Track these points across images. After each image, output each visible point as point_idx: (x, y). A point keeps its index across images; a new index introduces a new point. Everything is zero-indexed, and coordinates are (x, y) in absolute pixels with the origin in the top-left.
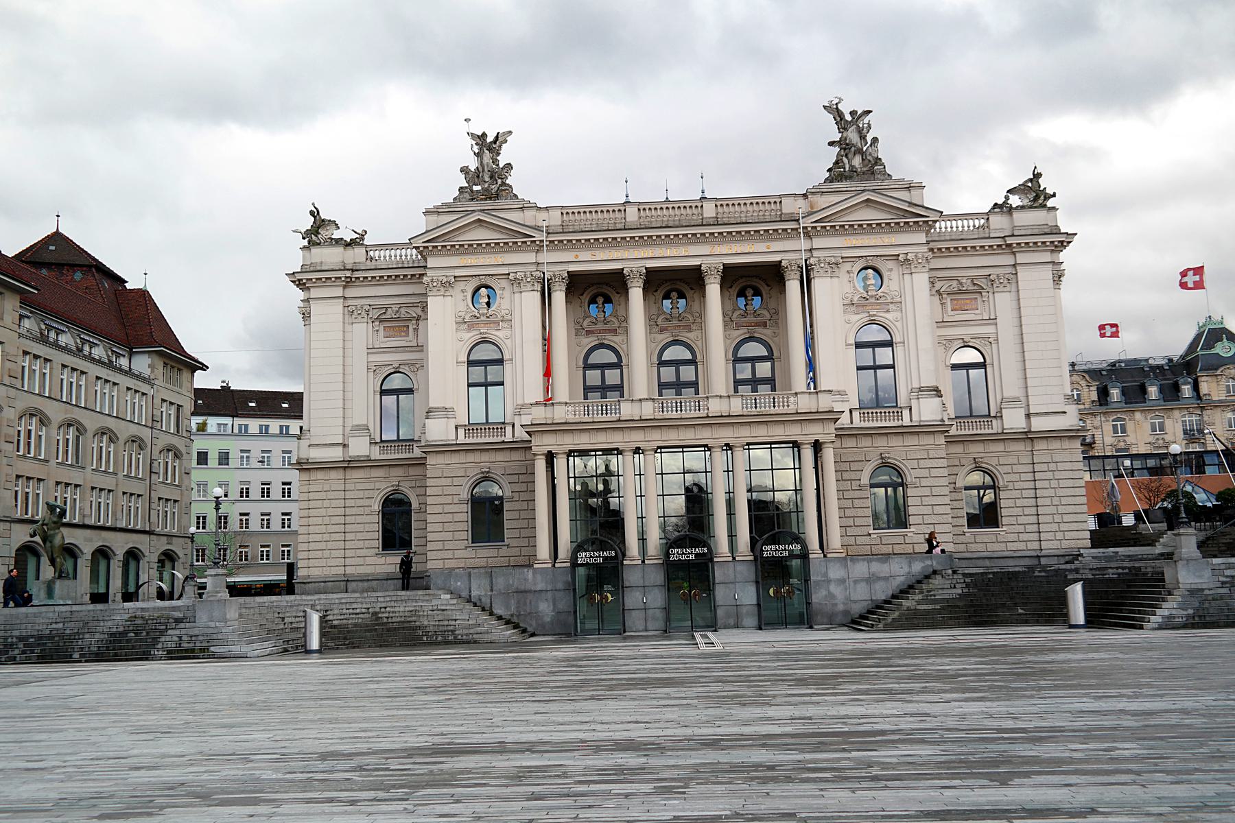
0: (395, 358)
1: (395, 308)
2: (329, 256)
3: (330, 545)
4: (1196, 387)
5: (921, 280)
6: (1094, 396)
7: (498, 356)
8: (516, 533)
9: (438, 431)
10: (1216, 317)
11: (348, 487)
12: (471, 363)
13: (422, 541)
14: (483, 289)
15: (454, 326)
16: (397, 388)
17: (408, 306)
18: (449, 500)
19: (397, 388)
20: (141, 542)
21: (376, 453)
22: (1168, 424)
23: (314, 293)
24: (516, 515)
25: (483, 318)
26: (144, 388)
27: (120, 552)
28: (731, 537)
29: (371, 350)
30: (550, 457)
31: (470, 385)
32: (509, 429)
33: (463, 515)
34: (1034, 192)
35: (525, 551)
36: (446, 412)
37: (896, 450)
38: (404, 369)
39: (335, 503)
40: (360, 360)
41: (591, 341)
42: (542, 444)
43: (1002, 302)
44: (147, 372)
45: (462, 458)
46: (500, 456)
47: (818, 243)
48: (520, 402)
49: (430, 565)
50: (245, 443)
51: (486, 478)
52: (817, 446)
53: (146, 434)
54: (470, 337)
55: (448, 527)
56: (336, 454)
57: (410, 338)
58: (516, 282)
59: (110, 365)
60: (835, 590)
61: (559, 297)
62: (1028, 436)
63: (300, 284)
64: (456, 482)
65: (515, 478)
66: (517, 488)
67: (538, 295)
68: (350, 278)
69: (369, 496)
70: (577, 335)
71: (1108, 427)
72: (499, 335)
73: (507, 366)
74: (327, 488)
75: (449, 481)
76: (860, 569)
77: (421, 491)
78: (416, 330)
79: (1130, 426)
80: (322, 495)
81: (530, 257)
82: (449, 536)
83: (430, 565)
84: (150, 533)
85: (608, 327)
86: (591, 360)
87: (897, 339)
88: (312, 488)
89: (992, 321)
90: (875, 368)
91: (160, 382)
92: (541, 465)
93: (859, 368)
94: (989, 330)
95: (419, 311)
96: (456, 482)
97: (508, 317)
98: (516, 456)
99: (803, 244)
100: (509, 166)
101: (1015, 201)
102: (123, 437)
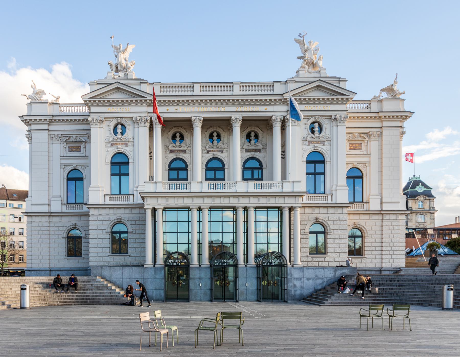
0: (73, 163)
1: (74, 136)
3: (42, 253)
7: (127, 161)
8: (134, 250)
11: (52, 225)
12: (113, 164)
13: (87, 253)
15: (105, 144)
17: (81, 136)
18: (100, 232)
24: (134, 241)
25: (119, 140)
31: (112, 175)
32: (131, 197)
35: (138, 259)
38: (79, 168)
39: (44, 233)
40: (57, 162)
41: (173, 156)
42: (149, 203)
46: (127, 211)
48: (137, 184)
49: (91, 264)
51: (119, 222)
54: (113, 150)
55: (100, 245)
56: (45, 209)
57: (82, 152)
64: (104, 223)
65: (134, 222)
66: (134, 227)
67: (147, 129)
70: (165, 152)
73: (131, 166)
74: (40, 225)
75: (100, 223)
77: (85, 228)
78: (85, 148)
80: (38, 229)
82: (100, 250)
83: (91, 264)
85: (182, 149)
86: (173, 166)
87: (327, 159)
88: (33, 225)
89: (368, 155)
90: (315, 174)
93: (307, 174)
95: (86, 138)
96: (104, 223)
97: (132, 140)
98: (135, 211)
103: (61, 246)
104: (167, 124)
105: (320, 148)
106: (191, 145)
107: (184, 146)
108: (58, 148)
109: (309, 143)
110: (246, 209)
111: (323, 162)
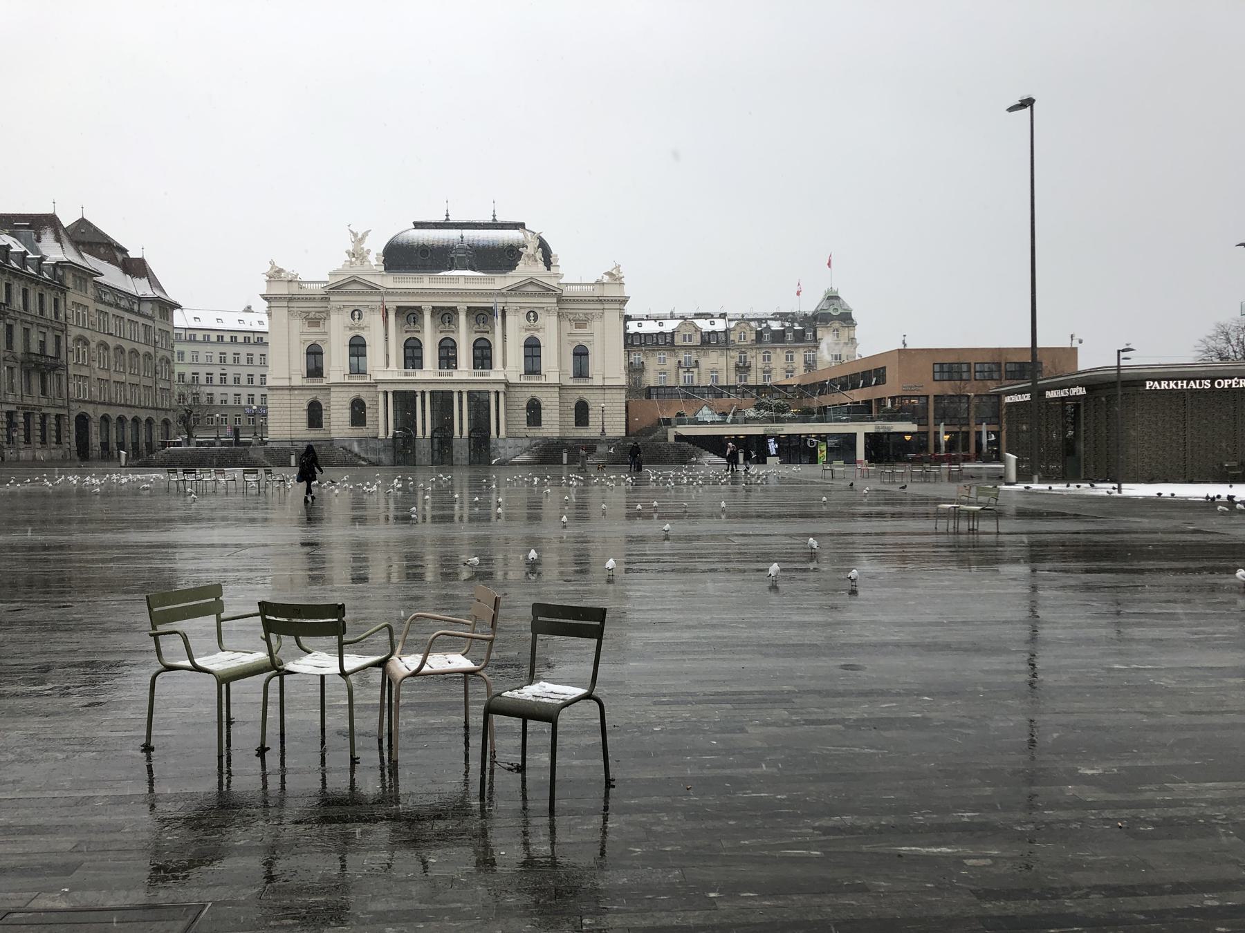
0: (314, 339)
4: (815, 334)
5: (554, 318)
6: (754, 337)
10: (835, 289)
12: (350, 345)
14: (356, 313)
16: (314, 353)
19: (314, 353)
20: (152, 414)
22: (796, 356)
23: (273, 304)
26: (150, 323)
27: (144, 420)
28: (461, 426)
29: (302, 333)
30: (386, 393)
33: (347, 414)
34: (615, 278)
37: (540, 394)
40: (296, 339)
42: (381, 388)
43: (596, 325)
44: (150, 312)
45: (347, 389)
47: (509, 299)
50: (195, 347)
52: (497, 393)
53: (151, 350)
56: (286, 383)
58: (372, 310)
59: (131, 311)
60: (502, 451)
61: (392, 317)
62: (603, 387)
63: (266, 299)
68: (291, 299)
69: (301, 403)
71: (760, 357)
72: (363, 334)
76: (510, 441)
79: (773, 357)
81: (379, 298)
84: (157, 409)
86: (409, 344)
89: (592, 334)
90: (533, 356)
91: (157, 318)
92: (381, 397)
99: (503, 300)
100: (369, 251)
101: (606, 279)
102: (141, 353)
103: (303, 418)
104: (399, 310)
105: (537, 335)
106: (422, 326)
107: (418, 327)
108: (298, 325)
109: (527, 330)
110: (460, 392)
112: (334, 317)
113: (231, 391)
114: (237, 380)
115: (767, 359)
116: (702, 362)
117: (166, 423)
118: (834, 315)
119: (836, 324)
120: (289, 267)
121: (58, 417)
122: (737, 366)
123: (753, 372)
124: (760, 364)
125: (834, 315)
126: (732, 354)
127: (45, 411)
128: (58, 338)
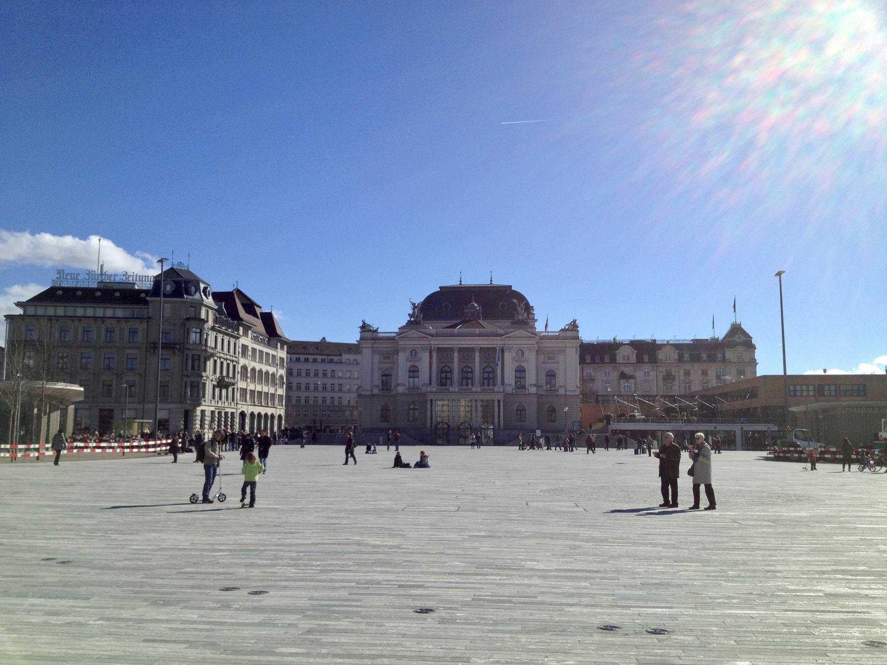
2: (369, 335)
6: (676, 357)
9: (401, 389)
12: (410, 371)
21: (380, 393)
22: (709, 372)
36: (403, 385)
43: (561, 358)
52: (499, 401)
54: (410, 364)
56: (369, 393)
61: (435, 355)
71: (682, 372)
72: (417, 364)
89: (558, 363)
92: (429, 402)
94: (556, 365)
111: (524, 371)
112: (400, 354)
113: (328, 395)
114: (316, 388)
115: (687, 373)
116: (639, 375)
117: (280, 416)
118: (739, 339)
119: (740, 348)
120: (374, 323)
121: (232, 414)
122: (664, 379)
123: (677, 383)
124: (682, 378)
125: (739, 339)
126: (660, 369)
127: (227, 410)
128: (234, 366)
